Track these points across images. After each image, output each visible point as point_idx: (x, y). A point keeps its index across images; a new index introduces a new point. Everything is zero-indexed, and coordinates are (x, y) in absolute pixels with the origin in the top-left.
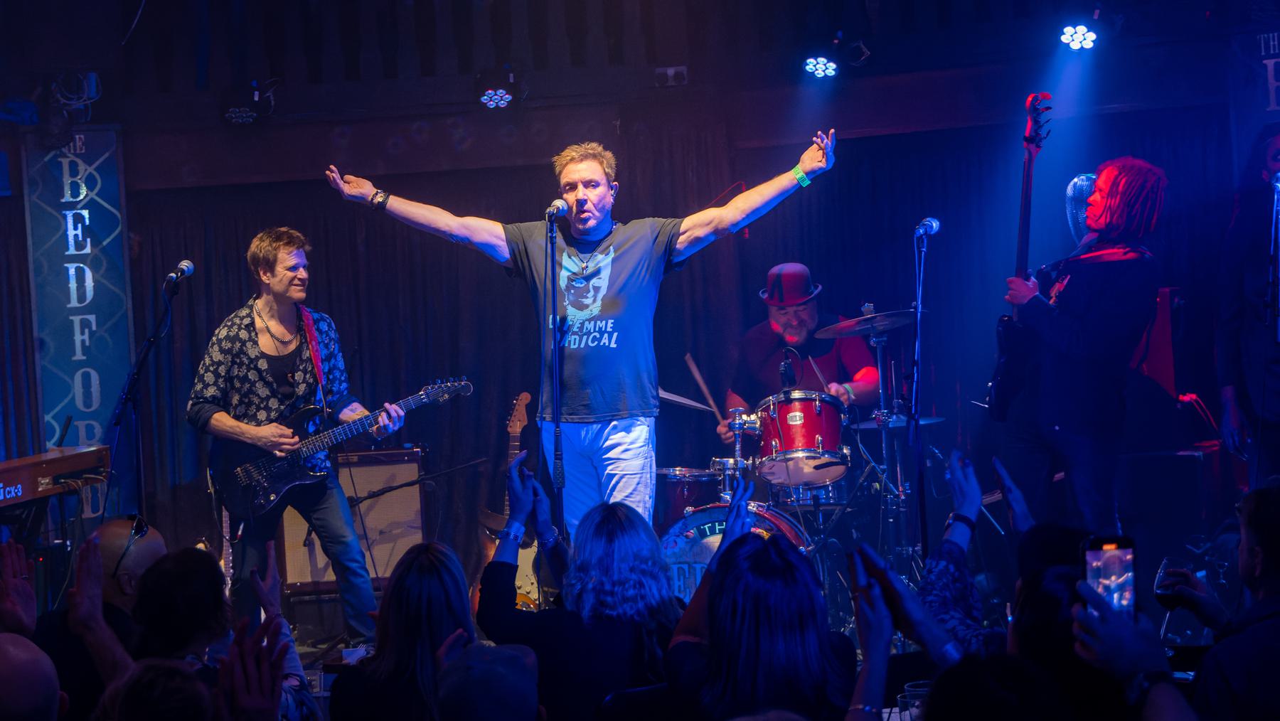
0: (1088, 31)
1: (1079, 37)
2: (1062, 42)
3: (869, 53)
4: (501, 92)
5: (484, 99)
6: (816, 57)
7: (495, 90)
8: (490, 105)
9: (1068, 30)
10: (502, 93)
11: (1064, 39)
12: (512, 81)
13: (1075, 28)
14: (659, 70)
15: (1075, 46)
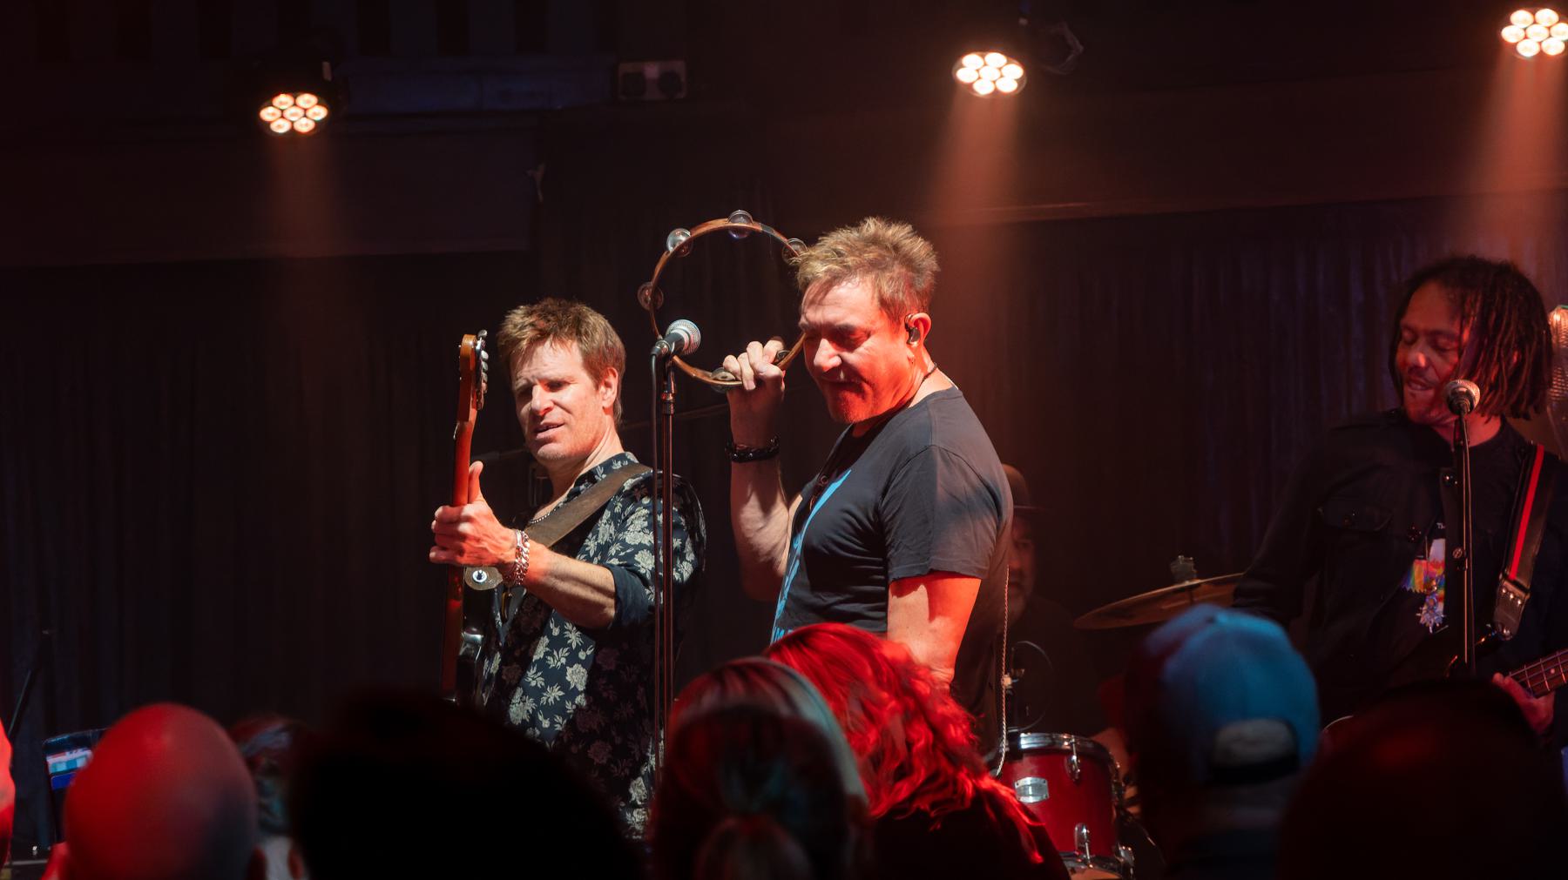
0: (1560, 21)
1: (1538, 32)
2: (1503, 40)
3: (1081, 48)
4: (307, 100)
5: (267, 114)
6: (983, 48)
7: (294, 91)
8: (279, 126)
9: (1520, 17)
10: (308, 102)
11: (1509, 34)
12: (327, 76)
13: (1534, 14)
14: (626, 67)
15: (1527, 50)
